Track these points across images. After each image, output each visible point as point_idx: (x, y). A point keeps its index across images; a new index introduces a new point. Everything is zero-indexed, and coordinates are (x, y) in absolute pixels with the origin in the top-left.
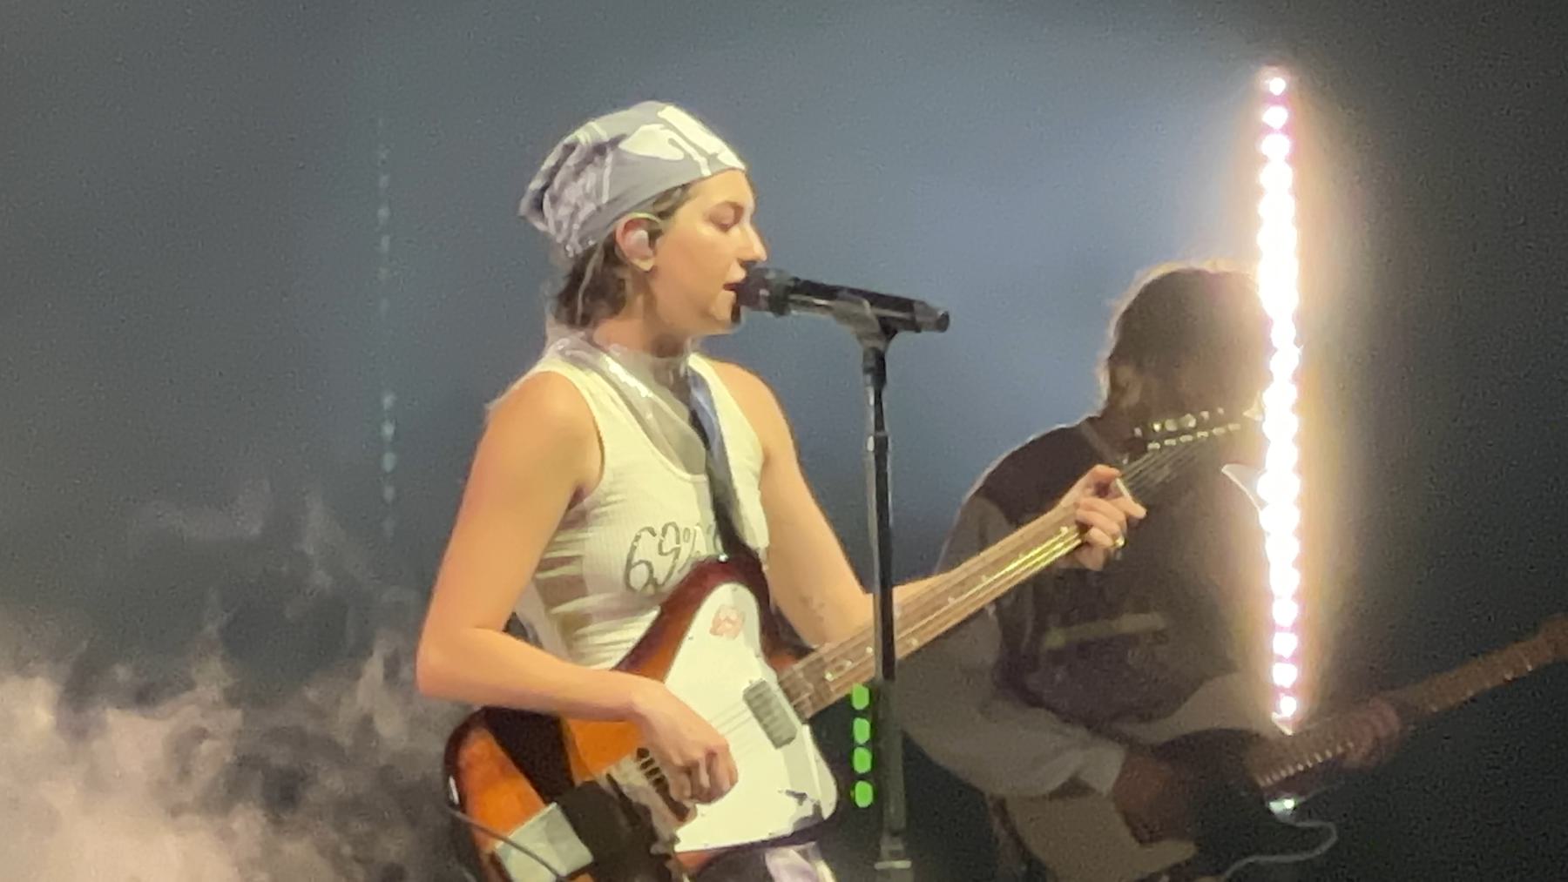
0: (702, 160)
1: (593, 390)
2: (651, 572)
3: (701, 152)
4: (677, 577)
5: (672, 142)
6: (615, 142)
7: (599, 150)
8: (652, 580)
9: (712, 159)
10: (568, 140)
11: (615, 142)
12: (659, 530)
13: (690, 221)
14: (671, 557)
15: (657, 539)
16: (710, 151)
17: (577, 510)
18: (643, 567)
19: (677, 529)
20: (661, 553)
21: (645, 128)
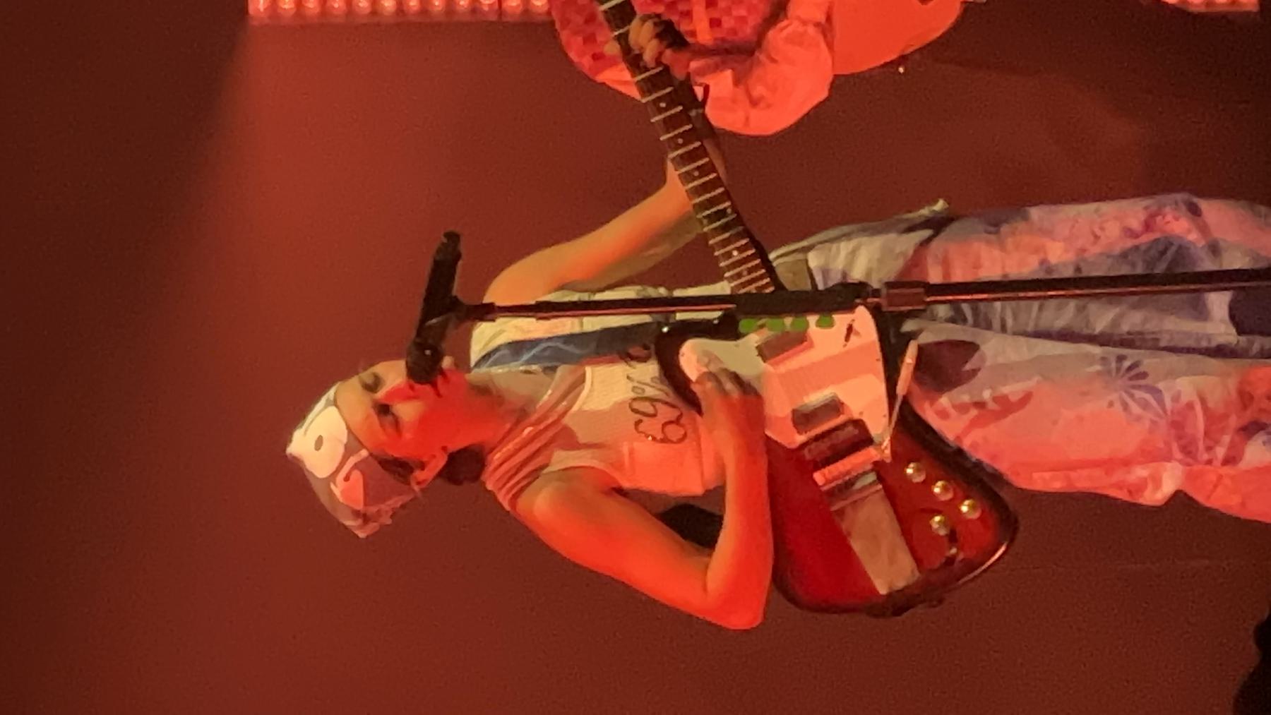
0: (352, 461)
2: (671, 422)
4: (672, 398)
6: (357, 514)
7: (366, 519)
8: (677, 422)
9: (349, 451)
11: (357, 514)
12: (638, 417)
14: (659, 405)
15: (645, 419)
16: (341, 450)
18: (670, 428)
19: (634, 399)
20: (654, 415)
21: (341, 500)
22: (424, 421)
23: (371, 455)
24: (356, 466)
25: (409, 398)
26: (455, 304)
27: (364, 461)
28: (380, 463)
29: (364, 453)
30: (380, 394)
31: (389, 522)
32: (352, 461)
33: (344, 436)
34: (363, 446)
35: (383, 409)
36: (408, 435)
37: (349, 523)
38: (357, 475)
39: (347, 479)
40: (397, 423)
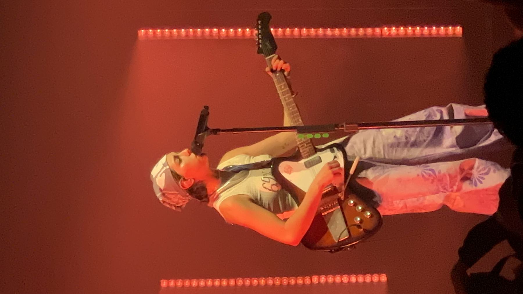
1: (225, 197)
3: (163, 168)
5: (161, 176)
6: (161, 190)
7: (163, 195)
9: (164, 165)
10: (162, 202)
16: (162, 166)
17: (256, 201)
21: (157, 183)
23: (170, 168)
25: (186, 155)
26: (207, 129)
27: (166, 169)
28: (172, 172)
29: (168, 167)
32: (165, 169)
34: (168, 165)
35: (176, 157)
36: (182, 165)
37: (159, 195)
38: (164, 174)
39: (161, 176)
40: (181, 161)
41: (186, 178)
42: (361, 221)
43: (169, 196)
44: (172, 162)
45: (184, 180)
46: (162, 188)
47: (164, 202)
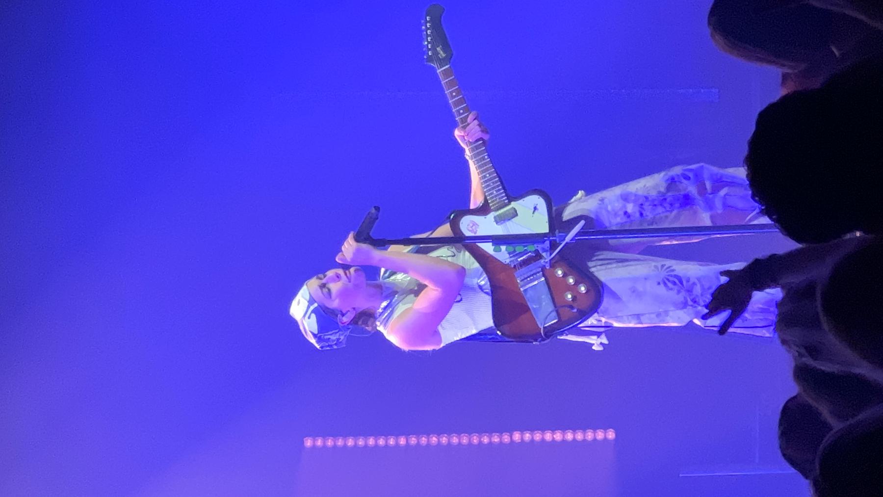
3: (308, 307)
5: (309, 318)
11: (315, 335)
13: (335, 304)
16: (306, 304)
22: (344, 294)
24: (313, 311)
29: (316, 305)
30: (324, 281)
31: (335, 347)
32: (312, 308)
33: (308, 297)
37: (313, 341)
38: (313, 316)
39: (309, 318)
40: (329, 290)
41: (344, 312)
42: (574, 298)
43: (326, 337)
44: (319, 294)
45: (343, 315)
46: (316, 332)
47: (322, 347)
